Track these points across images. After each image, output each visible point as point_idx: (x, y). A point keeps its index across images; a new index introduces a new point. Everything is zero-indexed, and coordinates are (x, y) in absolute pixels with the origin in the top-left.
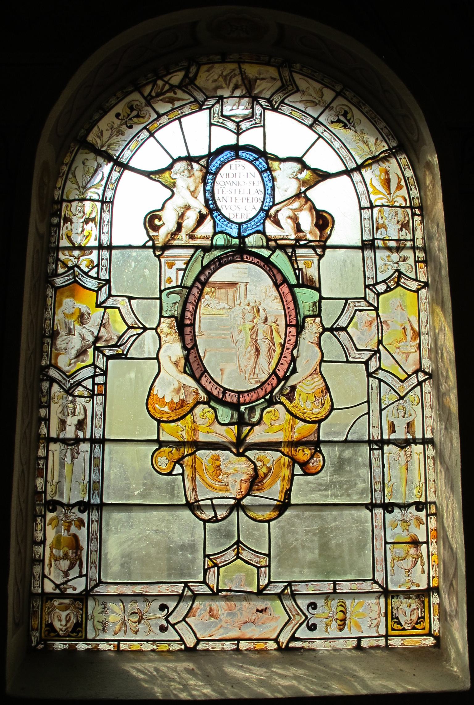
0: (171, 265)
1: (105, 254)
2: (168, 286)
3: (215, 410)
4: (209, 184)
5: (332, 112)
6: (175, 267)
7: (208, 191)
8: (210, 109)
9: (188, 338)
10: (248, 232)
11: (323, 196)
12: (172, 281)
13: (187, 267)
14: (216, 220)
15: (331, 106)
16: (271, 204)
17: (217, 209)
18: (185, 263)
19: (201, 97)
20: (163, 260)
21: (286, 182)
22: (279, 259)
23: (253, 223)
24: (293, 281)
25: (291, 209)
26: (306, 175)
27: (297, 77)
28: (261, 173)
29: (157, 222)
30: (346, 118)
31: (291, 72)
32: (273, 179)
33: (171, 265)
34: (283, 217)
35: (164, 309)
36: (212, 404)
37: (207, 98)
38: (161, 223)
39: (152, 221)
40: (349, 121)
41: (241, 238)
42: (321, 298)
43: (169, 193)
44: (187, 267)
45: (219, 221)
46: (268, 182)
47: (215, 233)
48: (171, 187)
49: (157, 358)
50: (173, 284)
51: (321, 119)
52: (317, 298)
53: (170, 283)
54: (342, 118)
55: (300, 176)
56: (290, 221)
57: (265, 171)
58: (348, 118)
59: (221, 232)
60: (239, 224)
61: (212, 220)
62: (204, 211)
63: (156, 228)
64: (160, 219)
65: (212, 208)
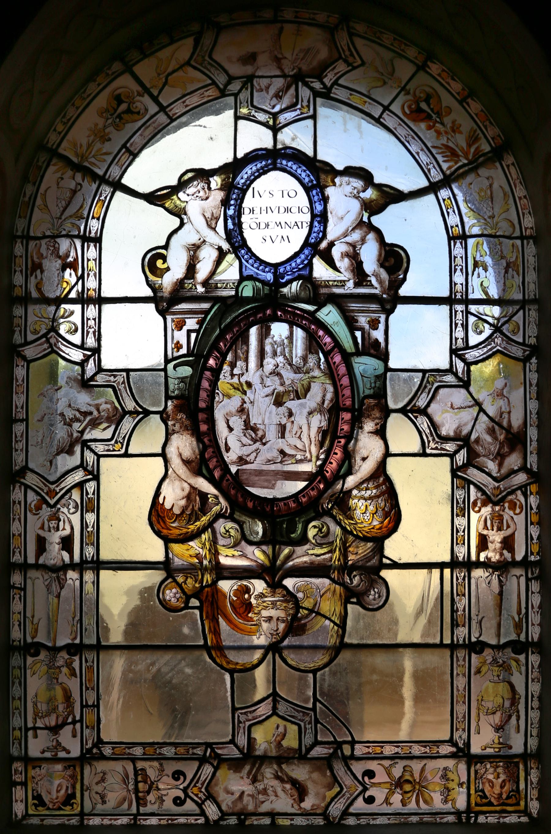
0: (180, 326)
1: (92, 311)
2: (176, 354)
3: (241, 524)
4: (232, 207)
5: (410, 97)
6: (185, 328)
7: (231, 216)
8: (236, 95)
9: (204, 428)
10: (287, 278)
11: (393, 223)
12: (181, 347)
13: (200, 328)
14: (243, 261)
15: (407, 87)
16: (321, 234)
17: (244, 244)
18: (197, 323)
19: (221, 80)
20: (169, 318)
21: (343, 202)
22: (329, 315)
23: (294, 265)
24: (348, 344)
25: (347, 243)
26: (370, 194)
27: (359, 42)
28: (308, 190)
29: (159, 263)
30: (429, 105)
31: (351, 35)
32: (325, 200)
33: (180, 326)
34: (336, 252)
35: (171, 387)
36: (237, 516)
37: (231, 79)
38: (165, 266)
39: (153, 262)
40: (432, 110)
41: (277, 284)
42: (387, 369)
43: (176, 222)
44: (200, 328)
45: (247, 262)
46: (317, 204)
47: (243, 278)
48: (179, 213)
49: (163, 455)
50: (184, 351)
51: (392, 108)
52: (381, 370)
53: (178, 351)
54: (424, 106)
55: (362, 195)
56: (346, 260)
57: (313, 187)
58: (432, 107)
59: (250, 278)
60: (276, 266)
61: (237, 261)
62: (226, 246)
63: (160, 273)
64: (165, 261)
65: (237, 242)
